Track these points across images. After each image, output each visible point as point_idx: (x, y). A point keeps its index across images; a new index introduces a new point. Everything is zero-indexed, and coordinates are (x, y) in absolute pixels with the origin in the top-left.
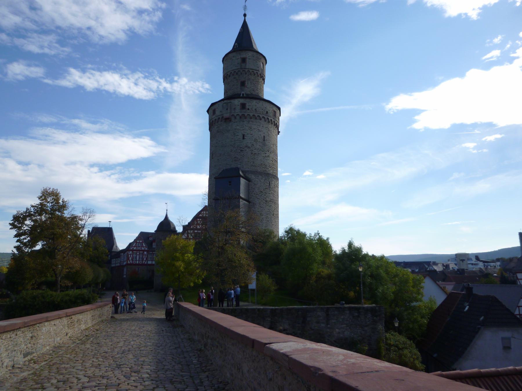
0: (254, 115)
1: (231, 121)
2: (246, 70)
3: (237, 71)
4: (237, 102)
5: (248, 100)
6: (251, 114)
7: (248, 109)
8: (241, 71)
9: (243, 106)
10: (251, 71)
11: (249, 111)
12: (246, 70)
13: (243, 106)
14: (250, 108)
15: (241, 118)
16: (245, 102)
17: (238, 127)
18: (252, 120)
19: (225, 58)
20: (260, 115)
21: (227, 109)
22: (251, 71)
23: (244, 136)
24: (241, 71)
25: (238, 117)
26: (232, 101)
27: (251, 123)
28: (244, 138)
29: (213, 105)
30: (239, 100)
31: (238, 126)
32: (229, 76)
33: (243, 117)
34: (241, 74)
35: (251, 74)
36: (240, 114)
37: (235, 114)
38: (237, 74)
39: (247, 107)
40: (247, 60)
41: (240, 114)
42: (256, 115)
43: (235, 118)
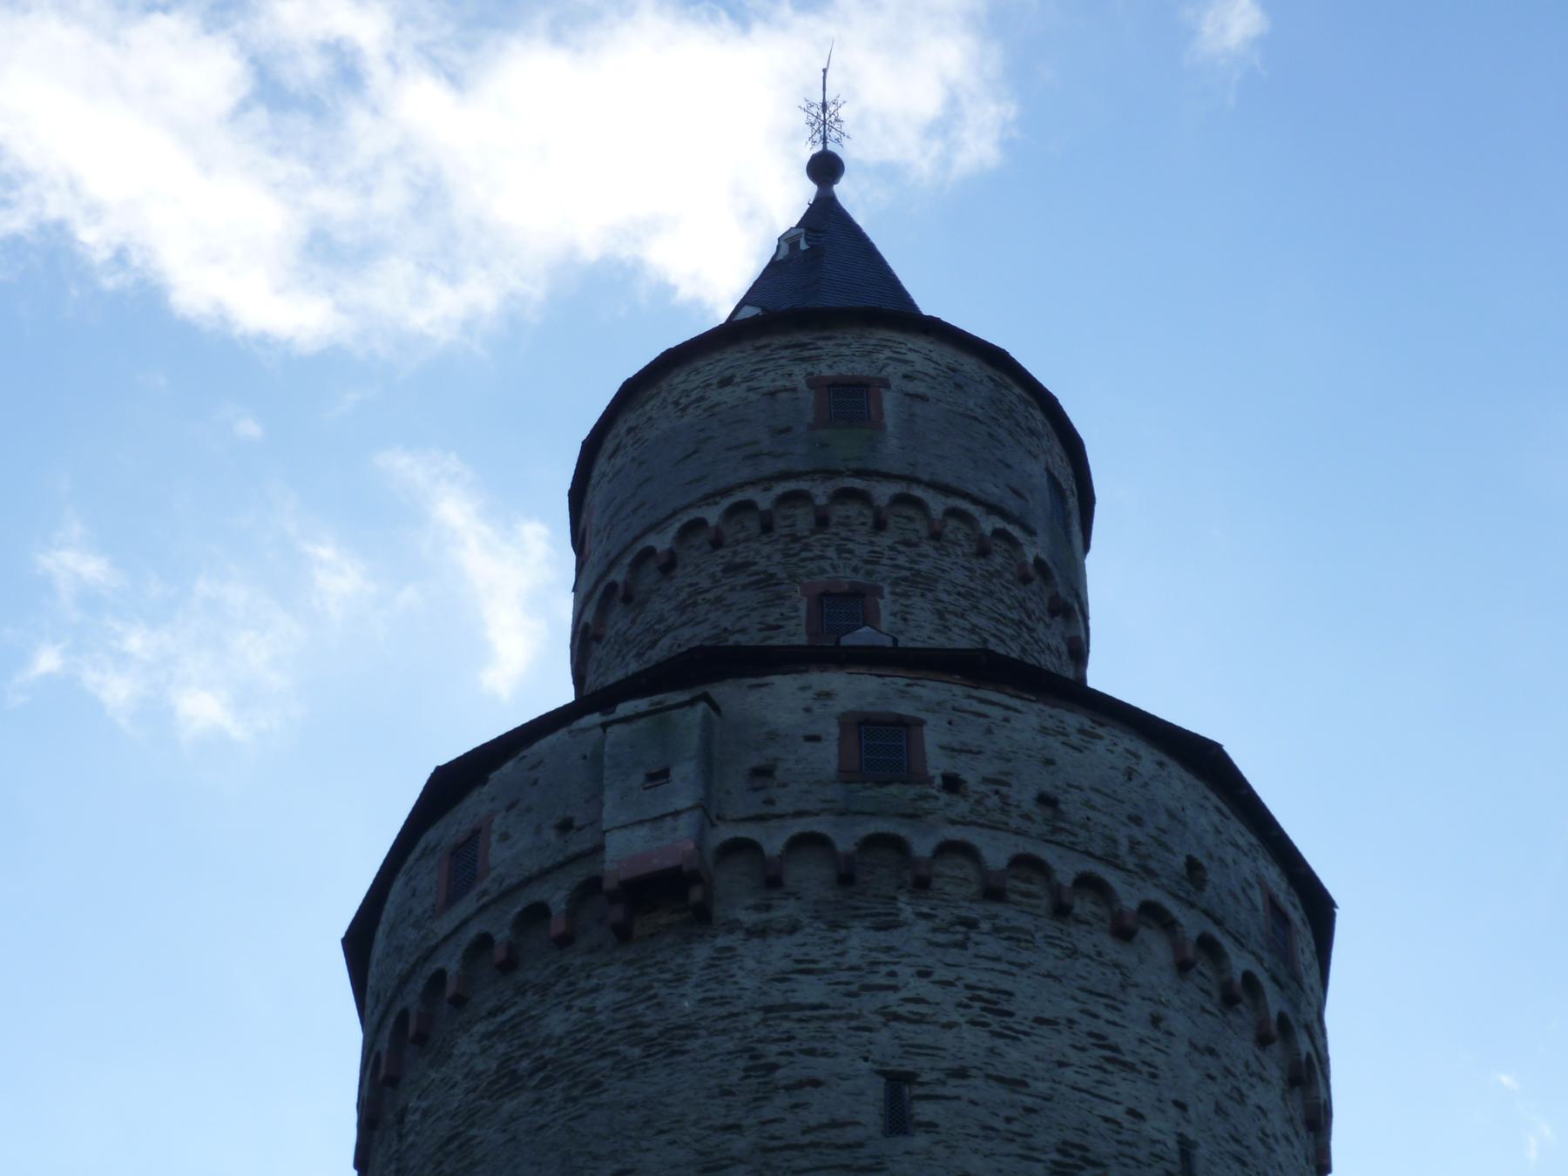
0: (1026, 864)
1: (702, 917)
2: (883, 492)
3: (764, 500)
4: (797, 710)
5: (932, 690)
6: (996, 852)
7: (952, 784)
8: (821, 492)
9: (881, 747)
10: (937, 504)
11: (962, 807)
12: (883, 492)
13: (881, 747)
14: (972, 773)
15: (846, 879)
16: (905, 708)
17: (810, 990)
18: (1007, 914)
19: (630, 419)
20: (1113, 878)
21: (659, 777)
22: (937, 504)
23: (897, 1082)
24: (821, 492)
25: (811, 876)
26: (729, 693)
27: (993, 946)
28: (898, 1121)
29: (449, 786)
30: (821, 679)
31: (807, 968)
32: (669, 565)
33: (874, 875)
34: (822, 522)
35: (936, 536)
36: (845, 839)
37: (773, 842)
38: (767, 528)
39: (937, 764)
40: (889, 401)
41: (845, 839)
42: (1066, 869)
43: (774, 882)
